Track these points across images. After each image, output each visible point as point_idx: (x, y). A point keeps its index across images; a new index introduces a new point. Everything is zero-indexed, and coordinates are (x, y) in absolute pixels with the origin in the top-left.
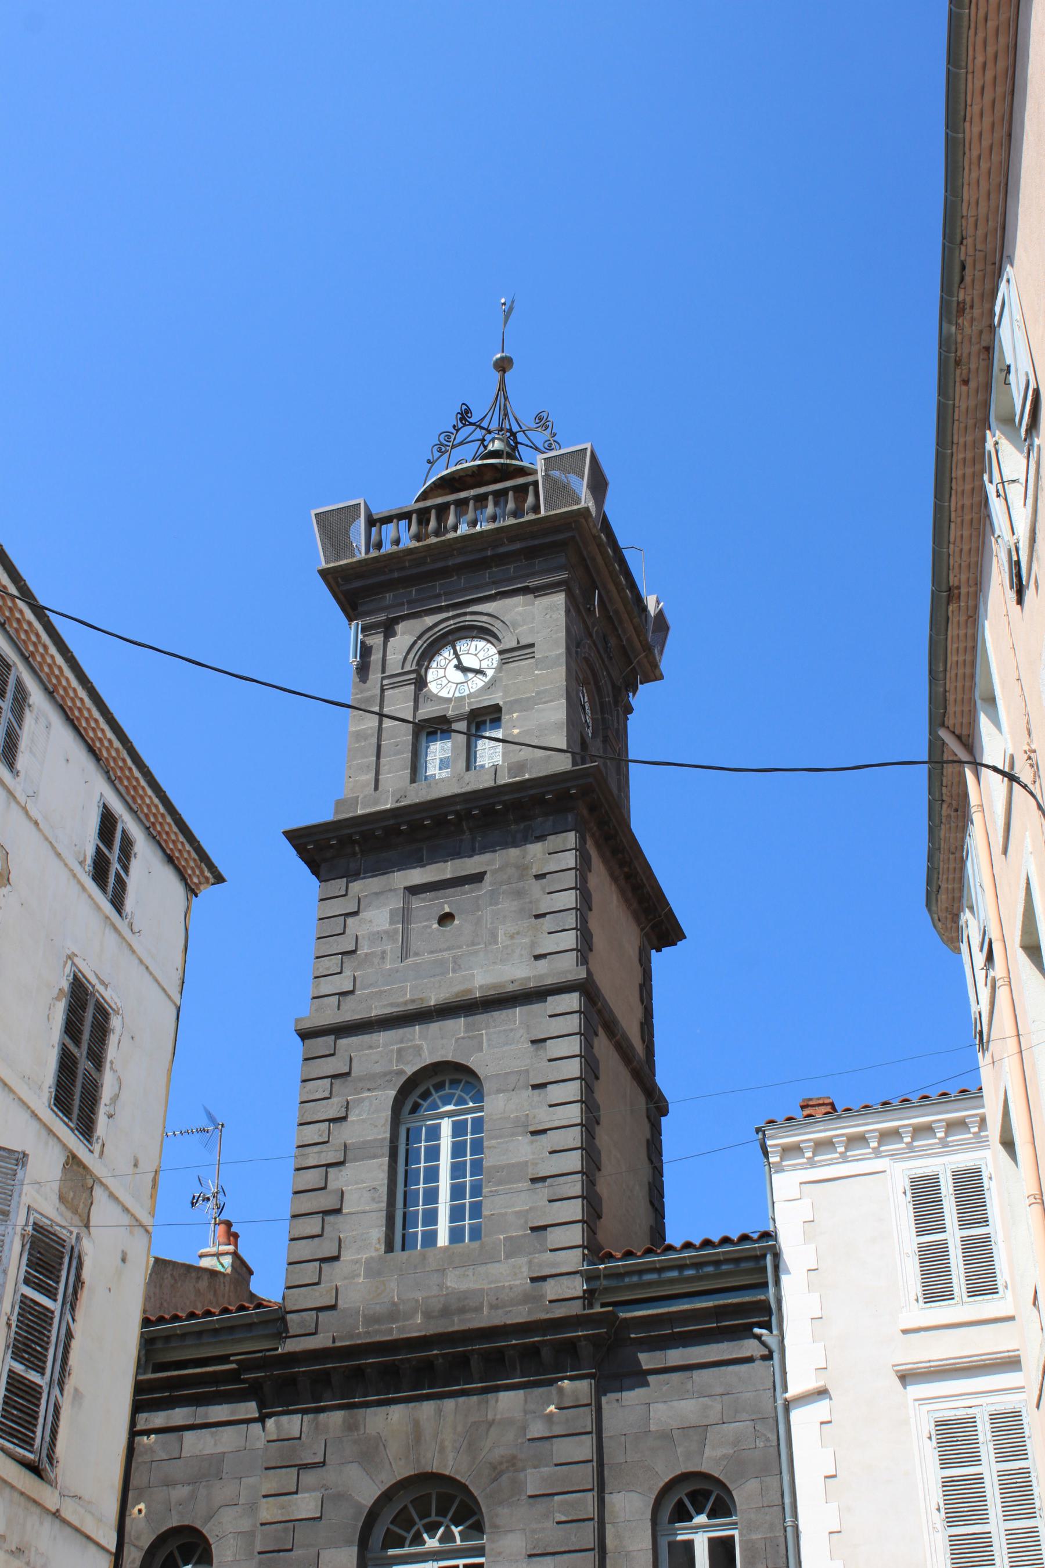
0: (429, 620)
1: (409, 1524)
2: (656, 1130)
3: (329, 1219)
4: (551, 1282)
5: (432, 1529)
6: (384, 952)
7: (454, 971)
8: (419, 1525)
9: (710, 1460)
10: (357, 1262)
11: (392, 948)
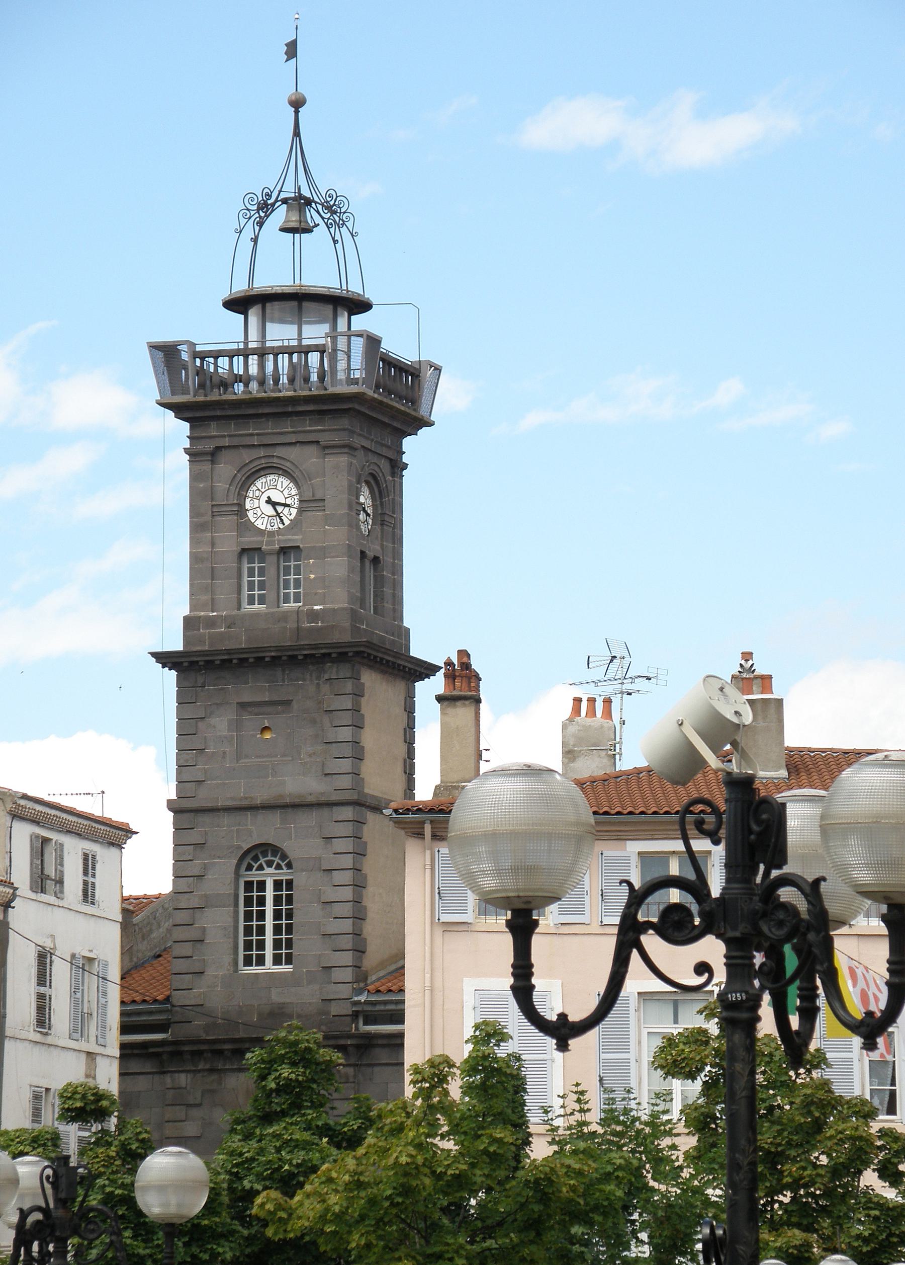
3: (198, 945)
4: (333, 1003)
6: (224, 753)
7: (272, 776)
10: (216, 976)
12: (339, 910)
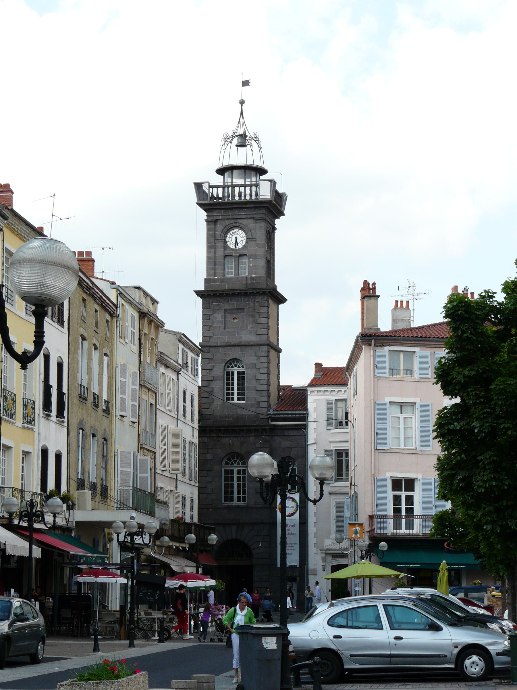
0: (227, 222)
1: (230, 460)
2: (279, 357)
5: (235, 462)
8: (232, 461)
9: (293, 454)
11: (222, 326)
12: (262, 382)
